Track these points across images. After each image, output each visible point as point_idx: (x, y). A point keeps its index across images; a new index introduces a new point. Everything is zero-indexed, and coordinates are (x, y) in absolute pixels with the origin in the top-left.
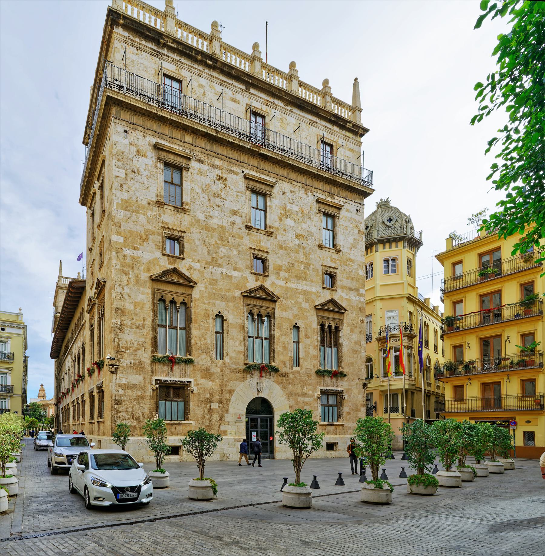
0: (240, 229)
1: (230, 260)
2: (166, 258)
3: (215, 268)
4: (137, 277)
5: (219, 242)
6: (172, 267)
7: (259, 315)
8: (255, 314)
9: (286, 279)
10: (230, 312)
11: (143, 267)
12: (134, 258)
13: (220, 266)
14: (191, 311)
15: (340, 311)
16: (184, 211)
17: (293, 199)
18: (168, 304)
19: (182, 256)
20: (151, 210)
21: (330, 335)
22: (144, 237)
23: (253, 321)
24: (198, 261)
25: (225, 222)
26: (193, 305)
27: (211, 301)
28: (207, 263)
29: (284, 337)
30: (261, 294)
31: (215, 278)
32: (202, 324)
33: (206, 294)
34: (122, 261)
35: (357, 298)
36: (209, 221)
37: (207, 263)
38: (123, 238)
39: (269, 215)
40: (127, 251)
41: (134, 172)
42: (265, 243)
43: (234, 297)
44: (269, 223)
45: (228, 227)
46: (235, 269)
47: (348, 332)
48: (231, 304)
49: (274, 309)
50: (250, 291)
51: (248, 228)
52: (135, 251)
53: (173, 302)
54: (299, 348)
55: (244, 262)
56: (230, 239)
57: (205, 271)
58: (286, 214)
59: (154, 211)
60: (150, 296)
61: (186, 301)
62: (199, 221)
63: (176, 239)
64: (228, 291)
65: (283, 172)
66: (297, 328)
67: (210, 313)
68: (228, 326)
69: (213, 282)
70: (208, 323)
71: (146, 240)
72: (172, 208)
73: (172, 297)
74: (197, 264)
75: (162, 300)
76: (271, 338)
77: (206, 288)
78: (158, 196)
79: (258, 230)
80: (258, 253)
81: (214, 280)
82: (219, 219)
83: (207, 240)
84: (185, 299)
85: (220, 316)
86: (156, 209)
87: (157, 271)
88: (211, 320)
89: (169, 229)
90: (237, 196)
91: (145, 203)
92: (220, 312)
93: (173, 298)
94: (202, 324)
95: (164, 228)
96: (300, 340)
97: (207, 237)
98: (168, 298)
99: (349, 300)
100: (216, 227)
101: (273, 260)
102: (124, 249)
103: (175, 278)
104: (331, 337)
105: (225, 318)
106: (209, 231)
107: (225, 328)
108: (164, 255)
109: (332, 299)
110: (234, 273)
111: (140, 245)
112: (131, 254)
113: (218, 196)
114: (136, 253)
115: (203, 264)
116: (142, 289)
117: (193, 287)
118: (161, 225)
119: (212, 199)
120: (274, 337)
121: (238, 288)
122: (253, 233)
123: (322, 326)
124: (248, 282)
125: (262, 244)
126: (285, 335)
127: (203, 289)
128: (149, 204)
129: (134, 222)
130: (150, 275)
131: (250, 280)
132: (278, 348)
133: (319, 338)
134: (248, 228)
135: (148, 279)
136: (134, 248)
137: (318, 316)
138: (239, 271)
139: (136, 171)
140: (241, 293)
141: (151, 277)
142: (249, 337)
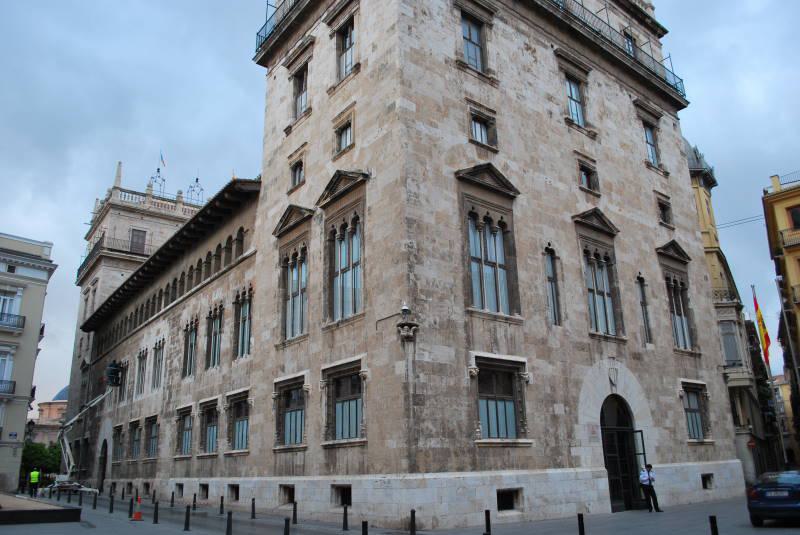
0: (559, 121)
2: (474, 147)
3: (537, 174)
4: (437, 170)
5: (537, 135)
6: (482, 162)
7: (597, 255)
8: (592, 253)
9: (618, 204)
11: (443, 157)
12: (430, 139)
13: (542, 171)
14: (513, 237)
15: (682, 259)
16: (493, 82)
17: (609, 98)
18: (481, 220)
19: (494, 147)
21: (677, 291)
22: (443, 109)
23: (589, 262)
24: (515, 159)
25: (543, 107)
26: (515, 229)
28: (526, 164)
29: (629, 293)
30: (595, 222)
32: (529, 261)
33: (530, 213)
34: (415, 140)
35: (696, 244)
36: (523, 103)
38: (414, 106)
39: (589, 110)
40: (421, 127)
41: (425, 13)
42: (589, 148)
43: (564, 222)
44: (590, 119)
45: (546, 116)
46: (561, 179)
47: (695, 292)
48: (561, 232)
49: (613, 247)
50: (585, 215)
51: (569, 122)
52: (432, 129)
53: (488, 220)
54: (647, 313)
55: (571, 171)
56: (550, 133)
58: (605, 113)
59: (453, 73)
60: (456, 205)
61: (505, 220)
62: (510, 100)
63: (484, 119)
64: (556, 210)
65: (596, 59)
66: (641, 280)
67: (538, 244)
68: (562, 268)
69: (537, 195)
70: (537, 259)
71: (446, 115)
72: (476, 75)
74: (514, 163)
75: (473, 215)
76: (614, 294)
77: (528, 202)
78: (456, 53)
79: (579, 127)
80: (584, 159)
81: (538, 192)
82: (534, 104)
84: (504, 216)
85: (550, 252)
86: (455, 71)
87: (464, 166)
88: (540, 256)
89: (475, 103)
90: (550, 76)
91: (441, 59)
92: (549, 244)
93: (488, 213)
94: (529, 261)
95: (469, 101)
96: (647, 300)
97: (523, 125)
98: (482, 212)
99: (688, 245)
100: (531, 112)
101: (603, 173)
102: (418, 123)
103: (488, 181)
104: (677, 301)
105: (557, 255)
106: (522, 116)
107: (559, 271)
108: (472, 141)
109: (674, 241)
110: (561, 186)
111: (439, 120)
112: (427, 131)
113: (529, 70)
114: (436, 132)
115: (522, 164)
116: (445, 192)
117: (512, 198)
118: (464, 96)
119: (522, 72)
121: (567, 208)
122: (574, 131)
123: (667, 279)
124: (578, 202)
125: (586, 148)
126: (631, 290)
127: (525, 203)
128: (446, 62)
129: (429, 84)
130: (456, 170)
131: (579, 198)
132: (626, 310)
133: (667, 299)
134: (569, 122)
135: (452, 176)
136: (431, 124)
137: (661, 265)
138: (565, 183)
139: (427, 12)
140: (573, 217)
141: (457, 173)
142: (591, 290)
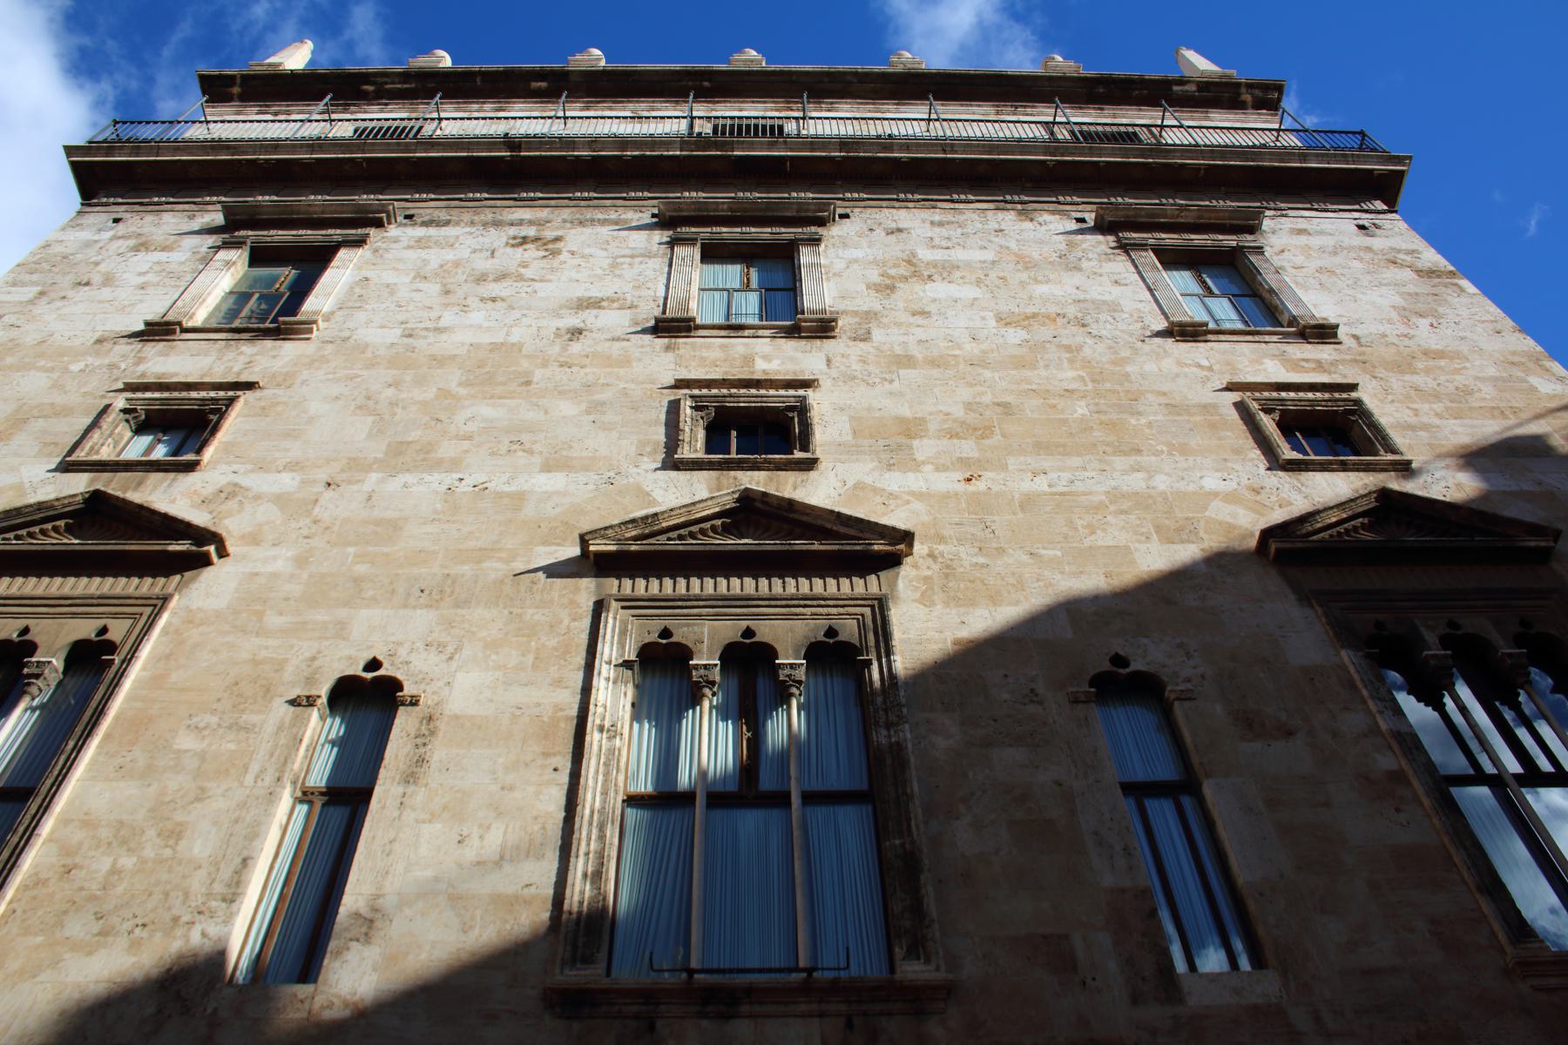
1: (525, 437)
5: (463, 391)
10: (467, 652)
20: (97, 354)
24: (293, 466)
27: (321, 616)
31: (389, 514)
37: (358, 465)
56: (538, 374)
57: (330, 493)
73: (21, 623)
77: (301, 561)
81: (378, 523)
83: (390, 392)
84: (110, 623)
90: (614, 266)
94: (186, 742)
120: (901, 763)
138: (586, 469)
